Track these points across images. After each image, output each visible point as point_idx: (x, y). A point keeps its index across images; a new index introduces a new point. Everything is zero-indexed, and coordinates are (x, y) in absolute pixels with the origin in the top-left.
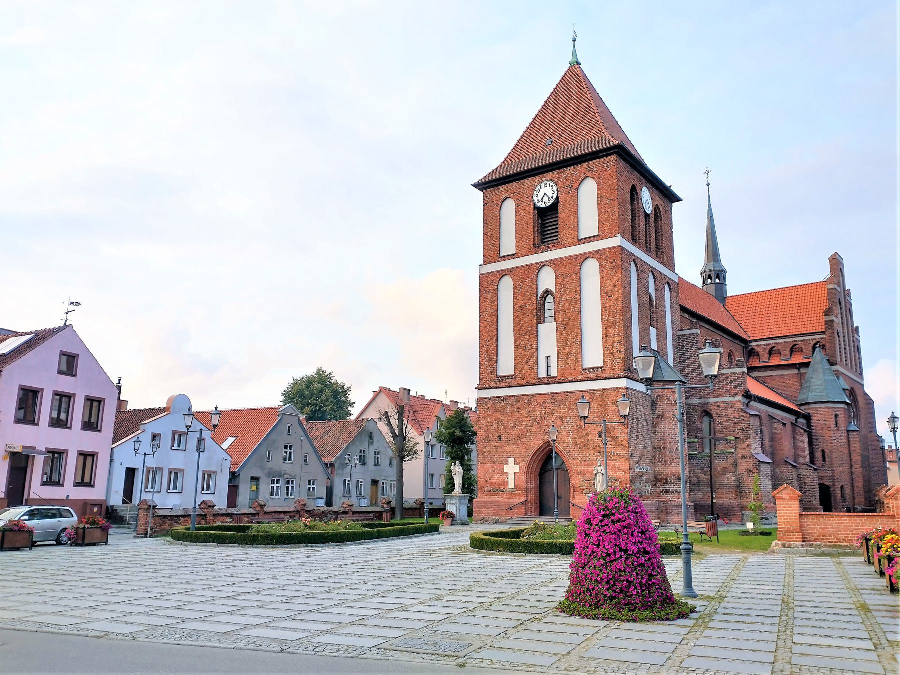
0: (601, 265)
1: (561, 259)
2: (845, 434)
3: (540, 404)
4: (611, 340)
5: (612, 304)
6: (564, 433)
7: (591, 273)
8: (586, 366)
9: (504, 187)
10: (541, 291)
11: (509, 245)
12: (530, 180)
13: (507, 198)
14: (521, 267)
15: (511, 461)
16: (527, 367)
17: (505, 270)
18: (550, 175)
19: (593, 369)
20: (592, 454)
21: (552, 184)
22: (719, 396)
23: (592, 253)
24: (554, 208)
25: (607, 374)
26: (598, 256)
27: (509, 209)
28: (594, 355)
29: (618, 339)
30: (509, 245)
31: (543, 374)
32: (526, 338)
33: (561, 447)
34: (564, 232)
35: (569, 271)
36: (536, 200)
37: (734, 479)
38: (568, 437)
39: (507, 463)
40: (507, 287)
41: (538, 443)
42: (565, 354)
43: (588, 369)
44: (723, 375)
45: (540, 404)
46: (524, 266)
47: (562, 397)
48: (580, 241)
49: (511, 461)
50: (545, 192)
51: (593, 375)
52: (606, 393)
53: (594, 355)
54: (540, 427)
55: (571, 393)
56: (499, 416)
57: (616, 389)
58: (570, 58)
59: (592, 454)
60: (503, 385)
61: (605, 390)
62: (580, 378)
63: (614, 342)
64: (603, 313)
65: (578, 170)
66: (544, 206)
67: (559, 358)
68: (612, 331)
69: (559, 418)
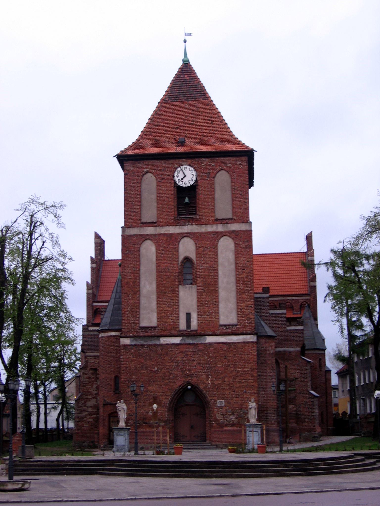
0: (236, 244)
1: (201, 233)
2: (324, 374)
3: (182, 352)
4: (244, 304)
5: (245, 275)
6: (204, 376)
8: (222, 322)
9: (146, 163)
10: (181, 258)
11: (149, 213)
12: (171, 161)
13: (148, 172)
14: (164, 234)
17: (148, 235)
18: (189, 161)
19: (229, 325)
20: (227, 392)
21: (191, 168)
23: (229, 232)
24: (193, 188)
25: (240, 331)
26: (233, 236)
27: (150, 182)
28: (228, 313)
29: (250, 303)
30: (149, 213)
31: (183, 326)
32: (167, 294)
33: (202, 387)
34: (202, 212)
35: (206, 244)
36: (176, 179)
37: (295, 409)
38: (207, 378)
40: (149, 250)
41: (179, 382)
42: (205, 312)
43: (225, 326)
44: (288, 330)
45: (182, 352)
48: (217, 220)
50: (186, 176)
51: (229, 331)
52: (239, 346)
53: (228, 313)
56: (143, 361)
57: (248, 343)
58: (183, 57)
60: (146, 334)
61: (239, 343)
62: (218, 332)
63: (247, 306)
64: (237, 282)
65: (214, 162)
66: (183, 185)
67: (199, 315)
68: (245, 296)
69: (200, 363)
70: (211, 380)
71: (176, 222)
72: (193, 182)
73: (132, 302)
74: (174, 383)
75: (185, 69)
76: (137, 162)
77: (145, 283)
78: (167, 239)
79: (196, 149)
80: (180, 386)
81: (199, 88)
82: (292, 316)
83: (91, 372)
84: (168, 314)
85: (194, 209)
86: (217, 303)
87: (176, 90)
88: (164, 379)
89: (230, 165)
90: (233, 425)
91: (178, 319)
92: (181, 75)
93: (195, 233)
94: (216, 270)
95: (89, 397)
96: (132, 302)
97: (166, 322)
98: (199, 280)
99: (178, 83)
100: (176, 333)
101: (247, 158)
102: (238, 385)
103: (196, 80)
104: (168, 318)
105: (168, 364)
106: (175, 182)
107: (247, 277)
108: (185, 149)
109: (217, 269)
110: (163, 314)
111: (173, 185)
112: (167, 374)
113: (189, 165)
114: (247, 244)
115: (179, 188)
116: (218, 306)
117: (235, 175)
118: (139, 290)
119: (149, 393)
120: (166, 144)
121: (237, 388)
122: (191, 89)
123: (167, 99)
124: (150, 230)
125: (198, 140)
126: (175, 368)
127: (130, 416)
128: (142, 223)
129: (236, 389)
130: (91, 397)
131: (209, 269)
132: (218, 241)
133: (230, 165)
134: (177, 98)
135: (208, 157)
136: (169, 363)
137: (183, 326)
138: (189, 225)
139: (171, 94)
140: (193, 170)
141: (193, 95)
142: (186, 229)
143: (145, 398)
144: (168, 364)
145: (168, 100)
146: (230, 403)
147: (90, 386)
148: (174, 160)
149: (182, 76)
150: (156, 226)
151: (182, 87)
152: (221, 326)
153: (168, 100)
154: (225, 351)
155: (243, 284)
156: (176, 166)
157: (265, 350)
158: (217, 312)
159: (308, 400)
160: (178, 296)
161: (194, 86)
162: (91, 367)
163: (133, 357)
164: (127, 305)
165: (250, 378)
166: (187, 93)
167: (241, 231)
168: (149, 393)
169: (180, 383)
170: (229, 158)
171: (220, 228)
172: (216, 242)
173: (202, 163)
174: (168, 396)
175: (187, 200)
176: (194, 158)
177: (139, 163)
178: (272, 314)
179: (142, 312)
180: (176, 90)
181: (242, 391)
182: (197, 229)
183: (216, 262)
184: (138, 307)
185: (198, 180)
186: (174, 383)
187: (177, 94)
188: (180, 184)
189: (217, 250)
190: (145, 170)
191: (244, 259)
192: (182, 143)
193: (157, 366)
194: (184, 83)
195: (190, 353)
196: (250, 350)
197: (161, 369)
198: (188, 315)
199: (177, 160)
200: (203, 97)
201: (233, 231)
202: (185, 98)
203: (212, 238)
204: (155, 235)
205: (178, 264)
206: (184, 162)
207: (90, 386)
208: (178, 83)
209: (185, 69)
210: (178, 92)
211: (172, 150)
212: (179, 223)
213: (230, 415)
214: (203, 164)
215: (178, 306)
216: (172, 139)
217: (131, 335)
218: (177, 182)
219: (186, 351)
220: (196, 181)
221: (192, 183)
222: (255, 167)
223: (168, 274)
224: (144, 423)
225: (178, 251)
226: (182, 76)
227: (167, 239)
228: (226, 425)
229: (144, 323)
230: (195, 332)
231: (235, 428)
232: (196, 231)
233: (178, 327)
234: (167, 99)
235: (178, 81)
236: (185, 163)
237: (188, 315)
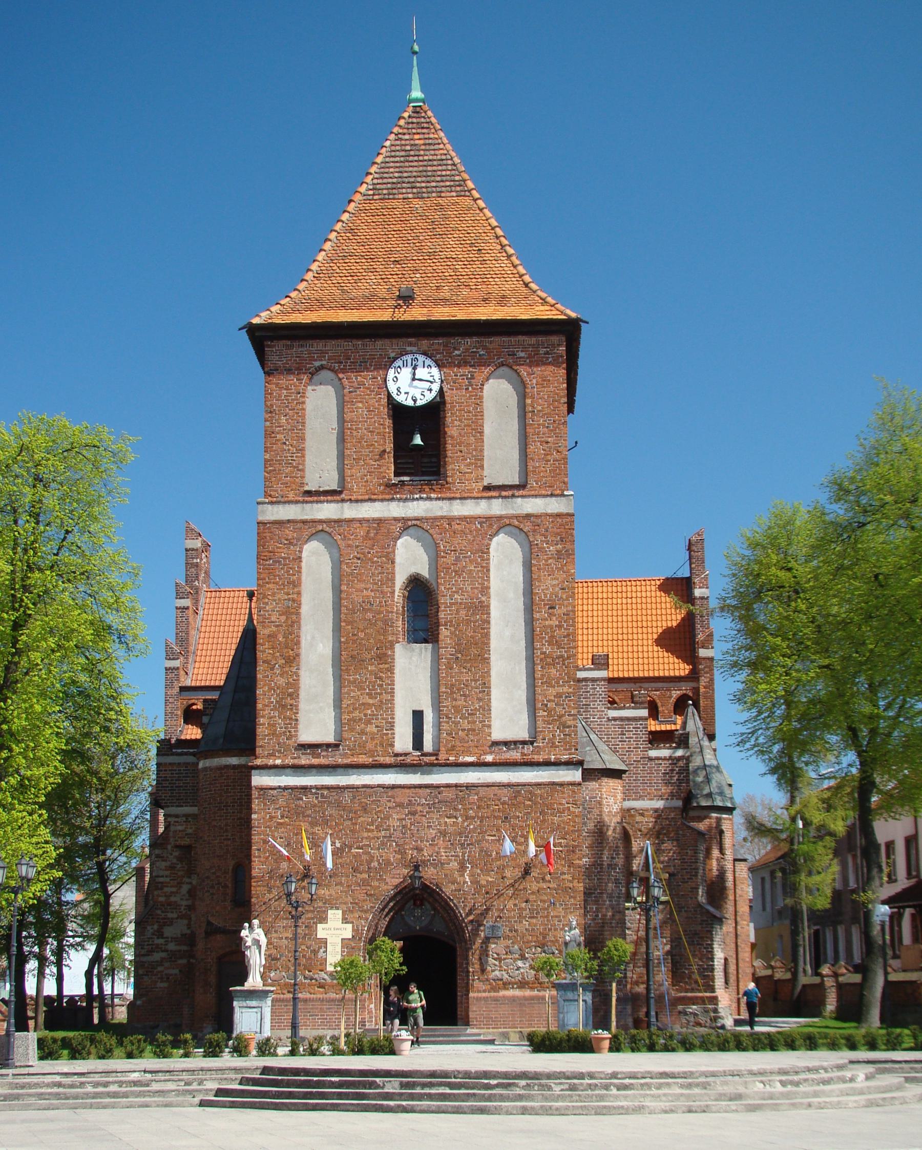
1: (450, 520)
3: (400, 805)
5: (554, 622)
6: (454, 865)
7: (505, 558)
9: (318, 345)
10: (400, 580)
12: (379, 343)
13: (322, 368)
14: (361, 521)
15: (335, 915)
16: (371, 728)
17: (321, 522)
18: (425, 343)
19: (515, 743)
22: (641, 798)
23: (517, 517)
26: (527, 527)
29: (566, 689)
33: (448, 890)
34: (455, 466)
38: (462, 868)
39: (324, 919)
42: (457, 709)
43: (506, 743)
44: (651, 759)
45: (400, 805)
46: (367, 520)
47: (449, 794)
48: (488, 488)
49: (335, 915)
51: (515, 755)
54: (402, 852)
55: (469, 787)
57: (561, 785)
59: (510, 905)
60: (315, 761)
62: (489, 758)
63: (559, 695)
66: (410, 403)
69: (443, 833)
70: (472, 875)
71: (391, 491)
72: (434, 394)
73: (282, 681)
74: (381, 879)
75: (415, 120)
76: (296, 344)
77: (313, 638)
78: (368, 532)
79: (442, 313)
80: (396, 886)
81: (450, 167)
82: (658, 729)
83: (176, 854)
84: (369, 712)
85: (434, 460)
86: (486, 688)
87: (391, 170)
88: (355, 870)
89: (522, 354)
90: (522, 984)
91: (391, 726)
92: (404, 134)
93: (436, 519)
94: (485, 608)
95: (170, 915)
96: (282, 681)
97: (363, 732)
98: (444, 632)
99: (398, 154)
100: (388, 760)
101: (564, 339)
102: (535, 886)
103: (441, 146)
104: (368, 722)
105: (366, 835)
106: (389, 396)
107: (560, 627)
108: (416, 313)
109: (488, 606)
110: (356, 714)
111: (384, 401)
112: (364, 857)
113: (425, 354)
114: (559, 546)
115: (398, 412)
116: (489, 694)
117: (534, 381)
118: (298, 655)
119: (321, 904)
120: (370, 299)
121: (533, 893)
122: (429, 168)
123: (371, 192)
124: (327, 511)
125: (446, 293)
126: (383, 844)
127: (273, 960)
128: (309, 493)
129: (532, 898)
130: (175, 915)
131: (468, 607)
132: (491, 540)
133: (522, 354)
134: (395, 191)
135: (470, 335)
136: (369, 831)
137: (403, 741)
138: (421, 498)
139: (380, 181)
140: (433, 364)
141: (434, 184)
142: (417, 508)
143: (310, 915)
144: (366, 835)
145: (374, 195)
146: (516, 931)
147: (174, 890)
148: (387, 341)
149: (407, 137)
150: (343, 501)
151: (407, 164)
152: (496, 743)
153: (374, 195)
154: (504, 803)
155: (550, 643)
156: (392, 355)
157: (600, 803)
158: (486, 709)
159: (699, 928)
160: (391, 670)
161: (435, 163)
162: (178, 843)
163: (282, 817)
164: (270, 689)
165: (565, 869)
166: (419, 179)
167: (547, 515)
168: (321, 904)
169: (396, 881)
170: (521, 338)
171: (497, 507)
172: (486, 542)
173: (455, 349)
174: (366, 911)
175: (418, 440)
176: (436, 336)
177: (302, 346)
178: (615, 719)
179: (303, 705)
180: (391, 170)
181: (543, 901)
182: (441, 508)
183: (485, 590)
184: (295, 695)
185: (445, 389)
186: (381, 879)
187: (395, 180)
188: (401, 399)
189: (489, 559)
190: (317, 364)
191: (555, 582)
192: (406, 298)
193: (340, 839)
194: (412, 153)
195: (419, 808)
196: (564, 801)
197: (350, 848)
198: (418, 716)
199: (394, 341)
200: (458, 189)
201: (528, 516)
202: (415, 190)
203: (477, 530)
204: (338, 521)
205: (393, 592)
206: (410, 344)
207: (174, 890)
208: (398, 154)
209: (415, 120)
210: (396, 175)
211: (385, 316)
212: (396, 493)
213: (515, 960)
214: (457, 352)
215: (392, 693)
216: (382, 291)
217: (278, 762)
218: (394, 396)
219: (410, 803)
220: (441, 392)
221: (429, 397)
222: (580, 362)
223: (369, 615)
224: (305, 978)
225: (393, 562)
226: (407, 137)
227: (368, 532)
228: (506, 985)
229: (306, 736)
230: (434, 758)
231: (528, 993)
232: (439, 513)
233: (392, 745)
234: (371, 192)
235: (398, 148)
236: (414, 349)
237: (418, 716)
